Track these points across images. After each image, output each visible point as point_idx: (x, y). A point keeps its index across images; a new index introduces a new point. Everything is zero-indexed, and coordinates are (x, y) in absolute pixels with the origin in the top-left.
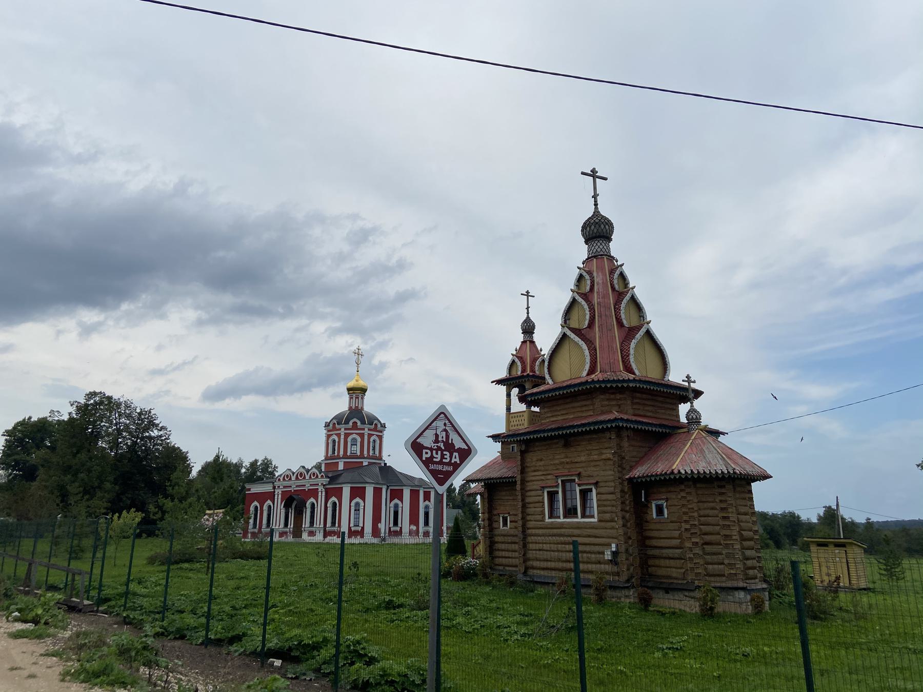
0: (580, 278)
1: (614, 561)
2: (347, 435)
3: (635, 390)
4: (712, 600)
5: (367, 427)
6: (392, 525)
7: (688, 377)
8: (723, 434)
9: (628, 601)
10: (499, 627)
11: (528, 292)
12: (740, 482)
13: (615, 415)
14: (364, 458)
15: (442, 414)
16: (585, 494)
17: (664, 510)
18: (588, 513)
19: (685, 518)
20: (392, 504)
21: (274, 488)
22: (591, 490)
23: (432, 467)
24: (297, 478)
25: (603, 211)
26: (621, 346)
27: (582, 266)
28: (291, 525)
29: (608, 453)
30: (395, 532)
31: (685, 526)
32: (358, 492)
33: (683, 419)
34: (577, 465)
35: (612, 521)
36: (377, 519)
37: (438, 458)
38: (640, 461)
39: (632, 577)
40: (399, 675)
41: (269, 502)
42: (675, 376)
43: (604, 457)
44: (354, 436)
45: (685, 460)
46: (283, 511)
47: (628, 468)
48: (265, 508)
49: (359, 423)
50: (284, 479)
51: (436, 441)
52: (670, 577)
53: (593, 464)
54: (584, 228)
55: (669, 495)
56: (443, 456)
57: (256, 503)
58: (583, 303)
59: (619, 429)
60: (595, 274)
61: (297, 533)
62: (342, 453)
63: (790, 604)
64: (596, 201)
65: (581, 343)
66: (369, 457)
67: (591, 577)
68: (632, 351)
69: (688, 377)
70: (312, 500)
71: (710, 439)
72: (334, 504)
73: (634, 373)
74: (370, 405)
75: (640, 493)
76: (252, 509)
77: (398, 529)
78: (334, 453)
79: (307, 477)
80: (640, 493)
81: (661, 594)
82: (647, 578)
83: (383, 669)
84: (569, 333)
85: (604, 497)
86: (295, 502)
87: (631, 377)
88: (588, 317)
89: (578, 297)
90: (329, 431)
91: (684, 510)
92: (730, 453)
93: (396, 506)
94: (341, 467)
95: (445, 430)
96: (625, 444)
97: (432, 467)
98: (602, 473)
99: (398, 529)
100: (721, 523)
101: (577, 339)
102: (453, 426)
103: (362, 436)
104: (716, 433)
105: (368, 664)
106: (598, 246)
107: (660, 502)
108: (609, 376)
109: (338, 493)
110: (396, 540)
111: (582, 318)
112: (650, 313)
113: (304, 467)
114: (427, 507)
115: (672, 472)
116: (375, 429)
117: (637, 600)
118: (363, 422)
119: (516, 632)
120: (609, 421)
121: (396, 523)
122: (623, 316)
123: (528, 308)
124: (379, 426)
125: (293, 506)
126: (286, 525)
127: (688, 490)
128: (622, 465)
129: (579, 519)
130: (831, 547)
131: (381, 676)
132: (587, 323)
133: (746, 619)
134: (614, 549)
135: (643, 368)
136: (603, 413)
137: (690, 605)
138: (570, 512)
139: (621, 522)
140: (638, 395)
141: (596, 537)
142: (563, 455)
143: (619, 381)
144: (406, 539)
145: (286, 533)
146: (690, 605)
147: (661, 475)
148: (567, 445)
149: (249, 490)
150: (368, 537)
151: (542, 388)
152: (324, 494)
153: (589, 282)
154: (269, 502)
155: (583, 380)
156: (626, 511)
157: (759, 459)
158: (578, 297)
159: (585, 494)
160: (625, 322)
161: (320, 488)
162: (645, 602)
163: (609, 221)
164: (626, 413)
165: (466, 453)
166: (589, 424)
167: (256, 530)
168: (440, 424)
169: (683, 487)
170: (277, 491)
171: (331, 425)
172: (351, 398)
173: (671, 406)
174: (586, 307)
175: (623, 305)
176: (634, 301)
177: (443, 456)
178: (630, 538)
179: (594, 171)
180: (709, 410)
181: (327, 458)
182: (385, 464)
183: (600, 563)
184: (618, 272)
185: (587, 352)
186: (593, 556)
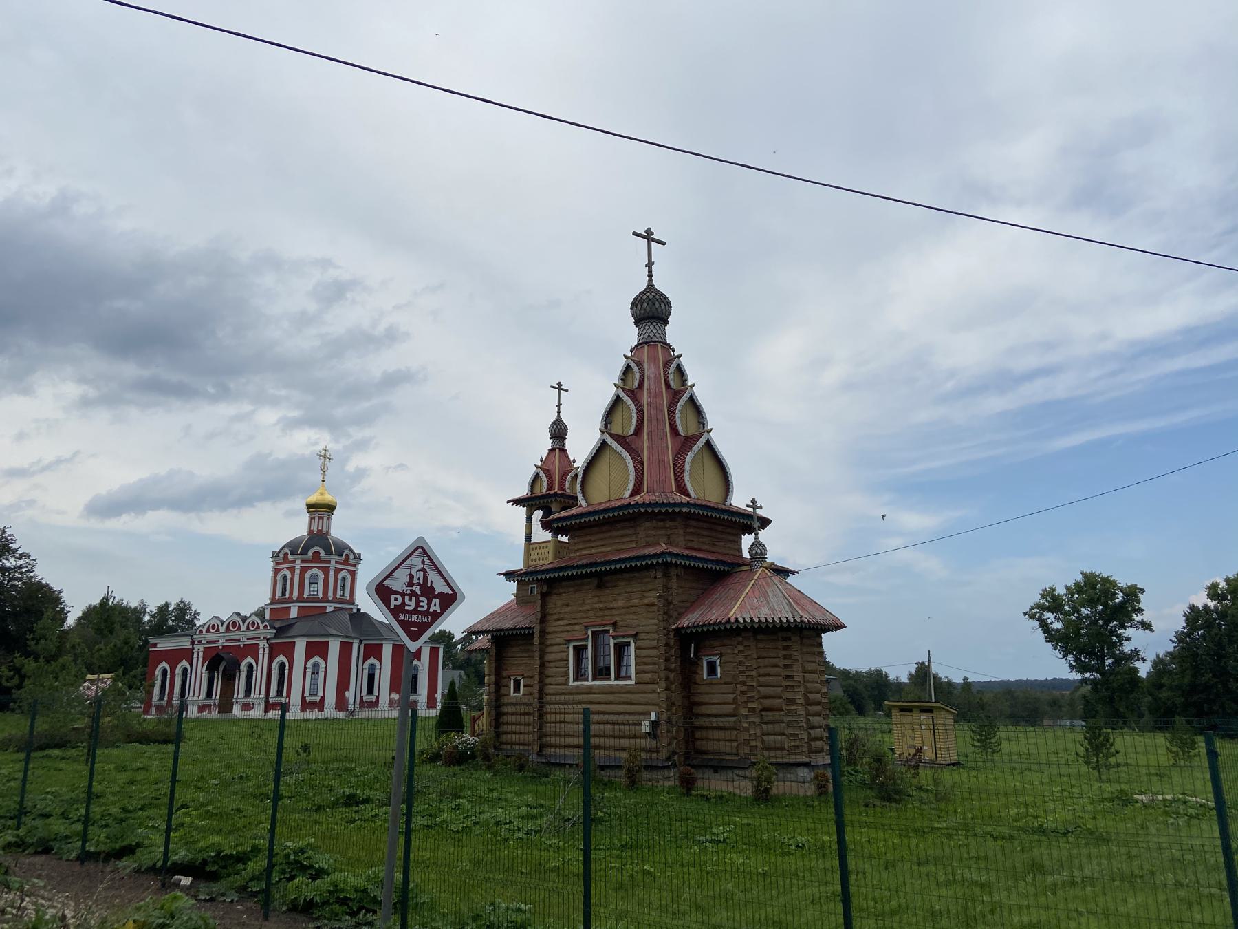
0: (627, 370)
1: (652, 735)
2: (304, 570)
3: (689, 516)
4: (769, 780)
5: (333, 559)
6: (364, 692)
7: (753, 501)
8: (793, 573)
9: (666, 784)
10: (497, 823)
11: (559, 384)
12: (808, 632)
13: (664, 547)
14: (328, 601)
15: (420, 549)
16: (621, 649)
17: (715, 670)
18: (623, 674)
19: (742, 678)
20: (366, 665)
21: (193, 643)
22: (628, 644)
23: (402, 617)
24: (228, 629)
25: (659, 286)
26: (674, 460)
27: (629, 354)
28: (217, 695)
29: (652, 597)
31: (741, 688)
32: (317, 649)
33: (746, 555)
34: (614, 612)
35: (653, 683)
36: (343, 685)
37: (411, 605)
38: (691, 606)
39: (674, 753)
40: (356, 890)
41: (185, 663)
42: (739, 501)
43: (646, 601)
45: (745, 605)
46: (205, 676)
47: (675, 615)
48: (178, 671)
49: (322, 553)
50: (208, 631)
51: (411, 584)
52: (720, 753)
53: (633, 610)
54: (634, 304)
55: (724, 650)
56: (418, 604)
57: (164, 665)
58: (630, 402)
59: (666, 565)
60: (646, 366)
61: (226, 705)
62: (295, 594)
63: (862, 783)
64: (650, 271)
65: (625, 454)
66: (335, 600)
67: (623, 755)
68: (687, 467)
69: (753, 501)
70: (250, 660)
71: (776, 579)
72: (282, 665)
73: (688, 495)
74: (339, 528)
75: (689, 646)
76: (158, 672)
77: (374, 698)
79: (243, 628)
80: (689, 646)
81: (709, 774)
82: (691, 753)
83: (334, 884)
84: (609, 440)
85: (644, 652)
86: (224, 664)
87: (685, 499)
88: (634, 421)
89: (622, 395)
91: (740, 668)
92: (798, 598)
93: (372, 667)
94: (294, 613)
95: (423, 570)
96: (674, 585)
97: (402, 617)
98: (644, 622)
99: (374, 698)
100: (784, 684)
101: (619, 449)
102: (434, 565)
103: (326, 571)
104: (783, 572)
105: (313, 878)
106: (651, 329)
107: (712, 659)
108: (657, 497)
109: (289, 650)
111: (627, 423)
112: (712, 420)
113: (238, 614)
115: (728, 621)
116: (346, 562)
117: (677, 783)
118: (329, 552)
119: (519, 829)
120: (655, 556)
121: (370, 691)
122: (678, 422)
123: (559, 405)
124: (352, 557)
126: (209, 695)
127: (746, 643)
128: (669, 611)
129: (612, 682)
130: (916, 714)
131: (330, 892)
132: (633, 428)
133: (806, 802)
134: (653, 719)
135: (700, 489)
136: (648, 545)
137: (742, 787)
138: (602, 672)
139: (663, 685)
140: (693, 523)
141: (632, 704)
142: (596, 599)
143: (669, 504)
146: (742, 787)
147: (715, 624)
148: (600, 586)
149: (155, 645)
150: (330, 711)
151: (573, 511)
152: (267, 651)
153: (637, 376)
154: (185, 663)
155: (624, 502)
156: (672, 671)
157: (832, 603)
158: (622, 395)
159: (621, 649)
160: (680, 429)
162: (688, 784)
163: (666, 298)
164: (676, 546)
165: (449, 600)
166: (629, 559)
167: (164, 703)
168: (416, 562)
169: (740, 639)
170: (196, 648)
171: (281, 556)
172: (312, 518)
173: (731, 538)
174: (633, 407)
175: (679, 408)
176: (692, 401)
177: (418, 604)
178: (673, 704)
179: (649, 232)
180: (777, 544)
181: (273, 601)
182: (359, 610)
183: (635, 737)
184: (674, 365)
185: (631, 467)
186: (627, 728)
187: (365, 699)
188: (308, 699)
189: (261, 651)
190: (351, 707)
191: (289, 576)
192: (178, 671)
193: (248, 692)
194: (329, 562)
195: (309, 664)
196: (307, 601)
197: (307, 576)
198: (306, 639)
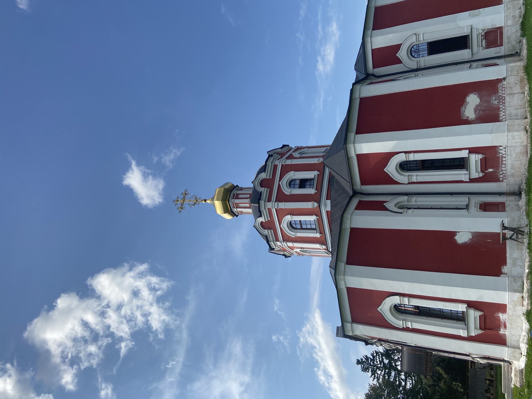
2: (287, 239)
6: (461, 175)
20: (402, 177)
30: (485, 164)
44: (284, 225)
74: (246, 180)
77: (475, 159)
93: (405, 166)
103: (281, 214)
121: (460, 164)
124: (263, 176)
187: (475, 175)
194: (270, 210)
196: (322, 232)
197: (292, 234)
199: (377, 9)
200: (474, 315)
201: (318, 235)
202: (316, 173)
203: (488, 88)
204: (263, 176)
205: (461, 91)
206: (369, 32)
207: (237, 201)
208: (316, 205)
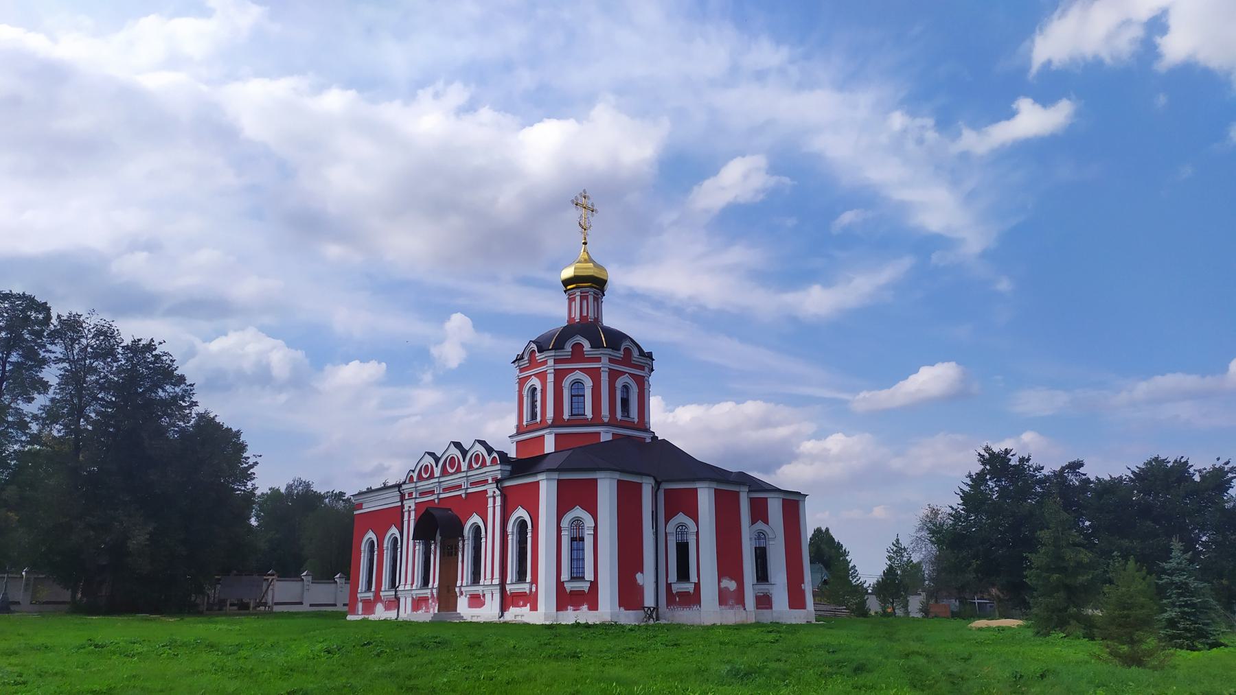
2: (559, 375)
5: (605, 355)
6: (673, 576)
21: (402, 498)
24: (444, 472)
28: (434, 583)
32: (575, 495)
36: (629, 561)
44: (578, 375)
46: (420, 548)
48: (387, 543)
50: (420, 478)
57: (371, 535)
61: (447, 598)
62: (550, 414)
66: (613, 423)
70: (476, 519)
72: (522, 525)
76: (364, 547)
77: (689, 587)
78: (534, 416)
79: (464, 467)
86: (441, 527)
90: (522, 370)
94: (549, 446)
103: (594, 374)
109: (530, 499)
110: (685, 616)
113: (458, 445)
114: (761, 535)
116: (627, 360)
118: (596, 344)
121: (683, 574)
124: (636, 353)
125: (438, 538)
126: (426, 582)
144: (710, 612)
145: (425, 599)
150: (607, 609)
152: (498, 499)
154: (394, 530)
161: (491, 489)
167: (370, 595)
170: (407, 504)
172: (571, 300)
181: (520, 430)
182: (655, 438)
188: (569, 587)
189: (490, 501)
190: (649, 601)
191: (539, 388)
192: (387, 543)
193: (476, 578)
194: (598, 360)
195: (565, 523)
197: (566, 383)
198: (556, 476)
199: (797, 502)
200: (585, 586)
201: (566, 416)
202: (636, 420)
203: (739, 598)
204: (636, 353)
205: (739, 578)
206: (782, 496)
207: (591, 299)
208: (606, 420)
